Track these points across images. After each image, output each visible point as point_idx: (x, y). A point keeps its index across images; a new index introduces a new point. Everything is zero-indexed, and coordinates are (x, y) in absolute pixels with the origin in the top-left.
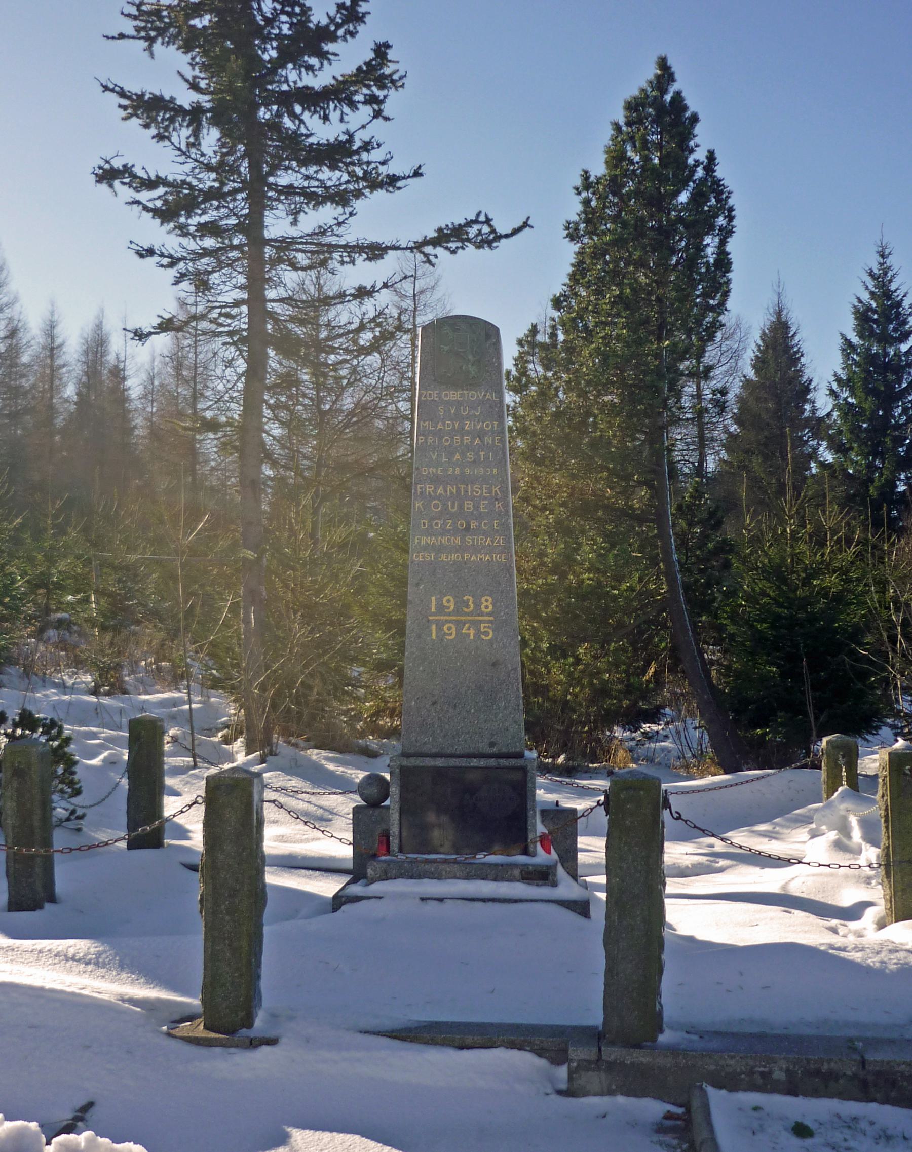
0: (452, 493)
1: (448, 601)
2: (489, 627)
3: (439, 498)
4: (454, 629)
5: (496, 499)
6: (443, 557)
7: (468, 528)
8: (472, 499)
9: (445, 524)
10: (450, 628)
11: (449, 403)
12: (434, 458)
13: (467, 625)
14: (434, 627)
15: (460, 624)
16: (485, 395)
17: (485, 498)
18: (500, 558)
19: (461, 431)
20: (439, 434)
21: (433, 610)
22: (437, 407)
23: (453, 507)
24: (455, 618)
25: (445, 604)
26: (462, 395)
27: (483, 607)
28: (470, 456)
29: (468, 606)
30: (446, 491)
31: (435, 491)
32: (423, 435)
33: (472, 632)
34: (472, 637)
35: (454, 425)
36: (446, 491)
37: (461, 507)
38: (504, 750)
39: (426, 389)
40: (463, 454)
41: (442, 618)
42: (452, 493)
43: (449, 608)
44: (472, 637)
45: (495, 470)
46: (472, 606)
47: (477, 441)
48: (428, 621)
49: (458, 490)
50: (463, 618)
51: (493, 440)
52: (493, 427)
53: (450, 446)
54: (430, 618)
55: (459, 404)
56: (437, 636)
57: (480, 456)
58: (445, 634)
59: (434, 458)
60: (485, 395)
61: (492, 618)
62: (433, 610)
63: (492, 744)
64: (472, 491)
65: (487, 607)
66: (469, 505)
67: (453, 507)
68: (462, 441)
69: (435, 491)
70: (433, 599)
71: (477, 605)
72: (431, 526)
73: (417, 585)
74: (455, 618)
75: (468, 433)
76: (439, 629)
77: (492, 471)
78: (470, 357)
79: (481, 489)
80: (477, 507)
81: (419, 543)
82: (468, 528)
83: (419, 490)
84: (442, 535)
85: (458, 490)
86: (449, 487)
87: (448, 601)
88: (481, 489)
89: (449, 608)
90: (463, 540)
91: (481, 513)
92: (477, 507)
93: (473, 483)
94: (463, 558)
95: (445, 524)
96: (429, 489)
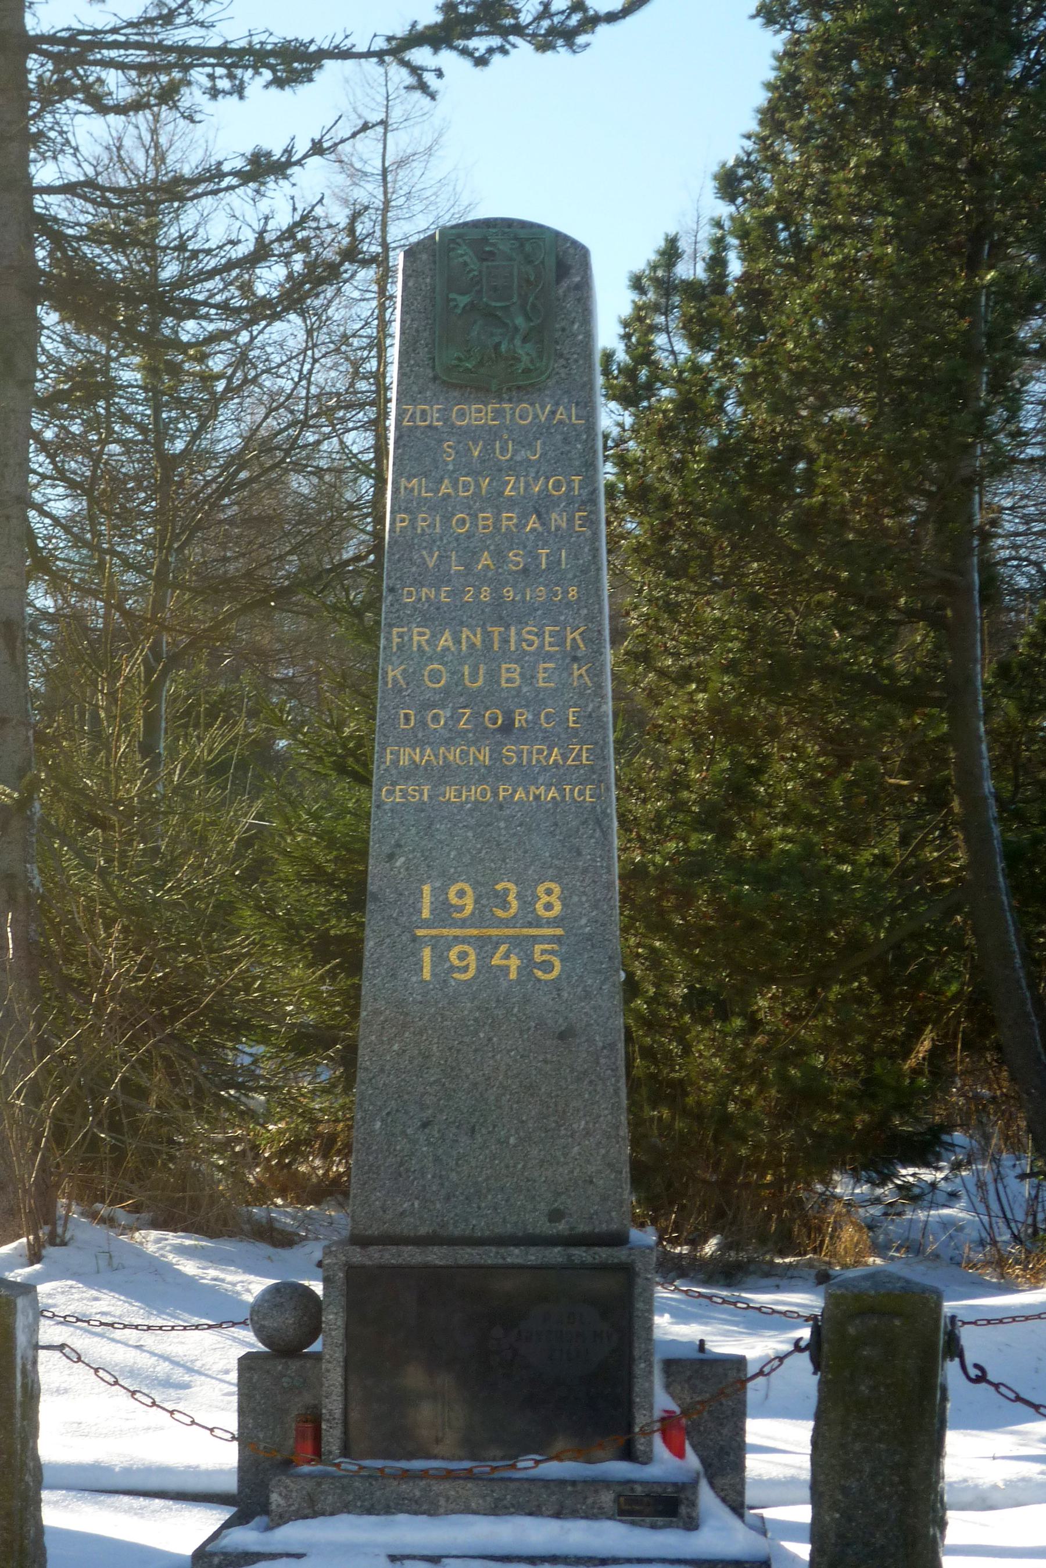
0: (472, 646)
1: (461, 894)
2: (552, 952)
3: (441, 657)
4: (472, 958)
5: (575, 659)
6: (450, 793)
7: (507, 728)
8: (520, 658)
9: (455, 718)
10: (463, 956)
11: (470, 434)
12: (431, 564)
13: (503, 948)
14: (427, 953)
15: (485, 946)
16: (553, 413)
17: (549, 657)
18: (581, 793)
19: (496, 501)
20: (443, 507)
21: (426, 914)
22: (440, 441)
23: (474, 677)
24: (475, 932)
25: (454, 900)
26: (498, 414)
27: (539, 906)
28: (516, 558)
29: (505, 905)
30: (458, 641)
31: (432, 642)
32: (406, 510)
33: (514, 962)
34: (513, 975)
35: (478, 486)
36: (458, 641)
37: (493, 676)
38: (583, 1228)
39: (414, 401)
40: (499, 556)
41: (445, 932)
42: (472, 646)
43: (461, 909)
44: (513, 975)
45: (573, 592)
46: (515, 904)
47: (533, 522)
48: (415, 939)
49: (487, 636)
50: (494, 932)
51: (571, 520)
52: (571, 489)
53: (469, 536)
54: (420, 932)
55: (492, 435)
56: (434, 974)
57: (537, 557)
58: (453, 968)
59: (431, 564)
60: (553, 413)
61: (559, 932)
62: (426, 914)
63: (555, 1216)
64: (520, 640)
65: (548, 907)
66: (510, 674)
67: (474, 677)
68: (497, 520)
69: (432, 642)
70: (427, 889)
71: (527, 902)
72: (423, 724)
73: (391, 857)
74: (475, 932)
75: (512, 503)
76: (440, 957)
77: (566, 592)
78: (520, 321)
79: (540, 635)
80: (529, 678)
81: (395, 762)
82: (507, 728)
83: (396, 640)
84: (448, 742)
85: (487, 636)
86: (466, 632)
87: (461, 894)
88: (540, 635)
89: (461, 909)
90: (496, 755)
91: (538, 691)
92: (529, 678)
93: (521, 622)
94: (495, 794)
95: (455, 718)
96: (419, 636)
